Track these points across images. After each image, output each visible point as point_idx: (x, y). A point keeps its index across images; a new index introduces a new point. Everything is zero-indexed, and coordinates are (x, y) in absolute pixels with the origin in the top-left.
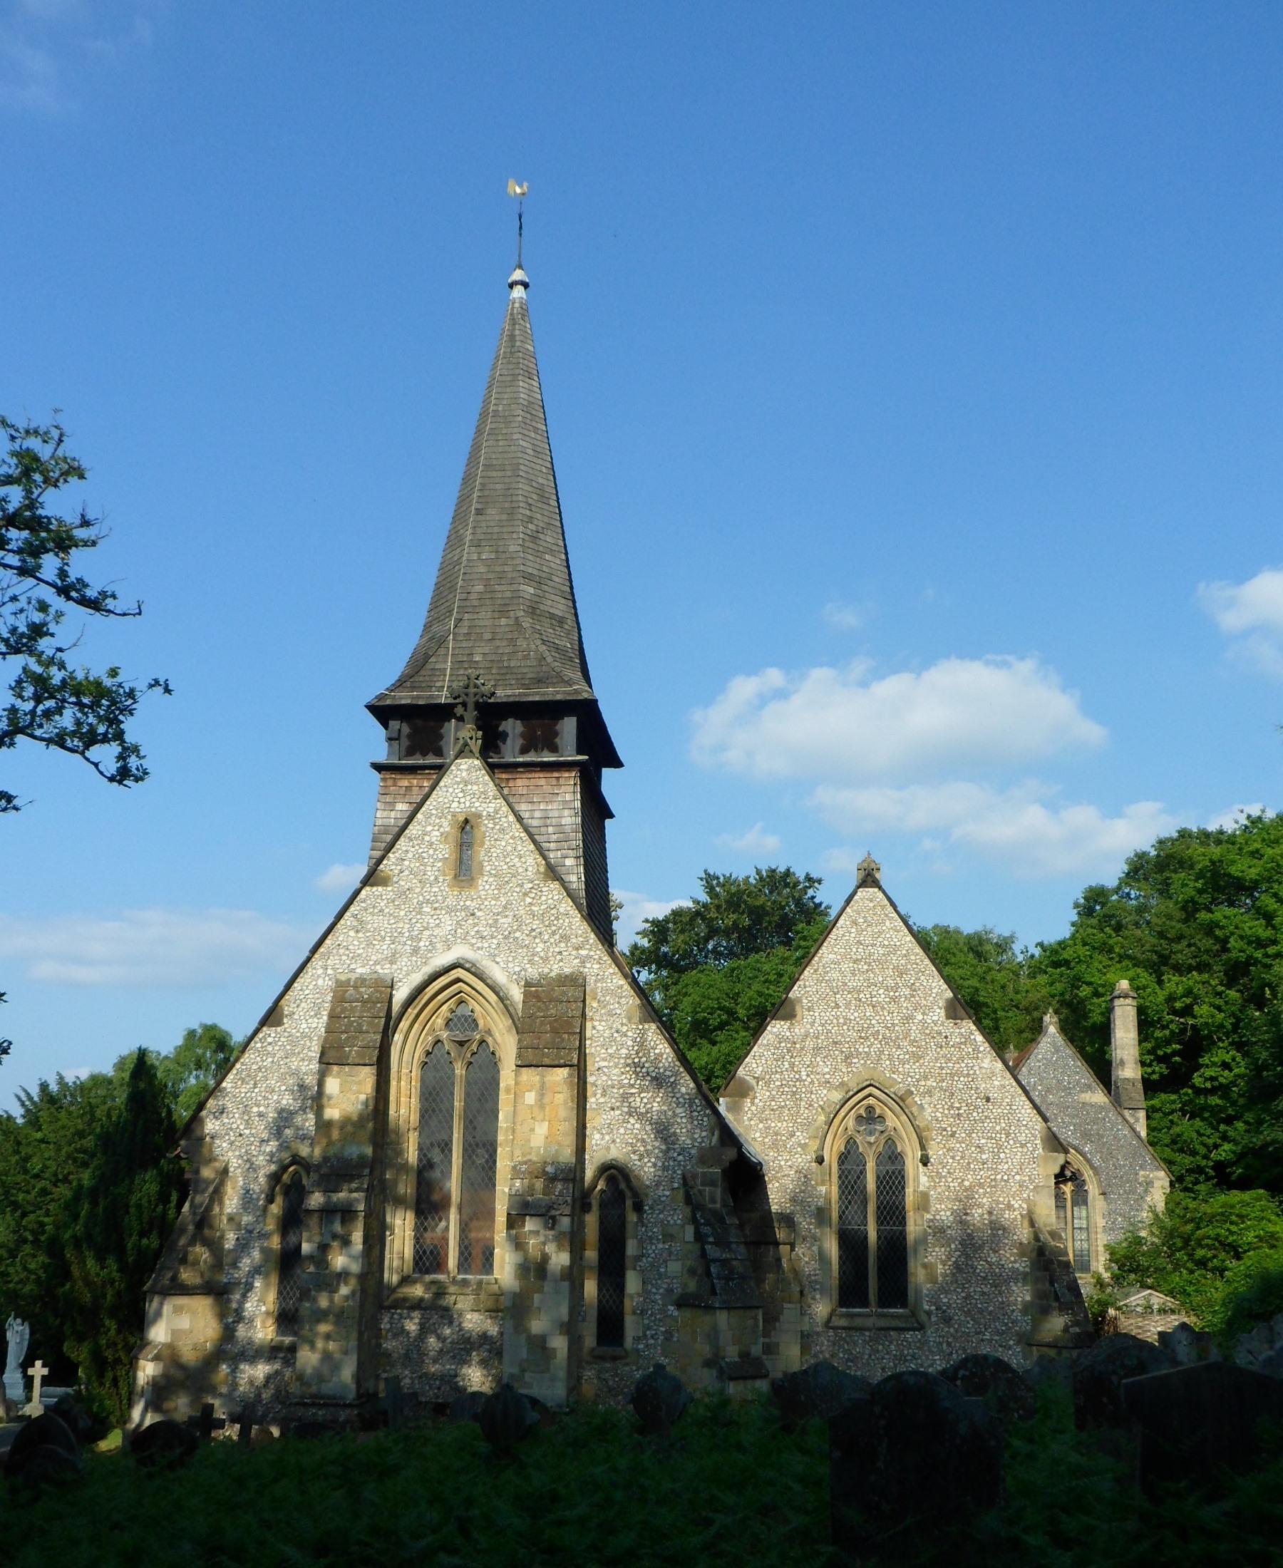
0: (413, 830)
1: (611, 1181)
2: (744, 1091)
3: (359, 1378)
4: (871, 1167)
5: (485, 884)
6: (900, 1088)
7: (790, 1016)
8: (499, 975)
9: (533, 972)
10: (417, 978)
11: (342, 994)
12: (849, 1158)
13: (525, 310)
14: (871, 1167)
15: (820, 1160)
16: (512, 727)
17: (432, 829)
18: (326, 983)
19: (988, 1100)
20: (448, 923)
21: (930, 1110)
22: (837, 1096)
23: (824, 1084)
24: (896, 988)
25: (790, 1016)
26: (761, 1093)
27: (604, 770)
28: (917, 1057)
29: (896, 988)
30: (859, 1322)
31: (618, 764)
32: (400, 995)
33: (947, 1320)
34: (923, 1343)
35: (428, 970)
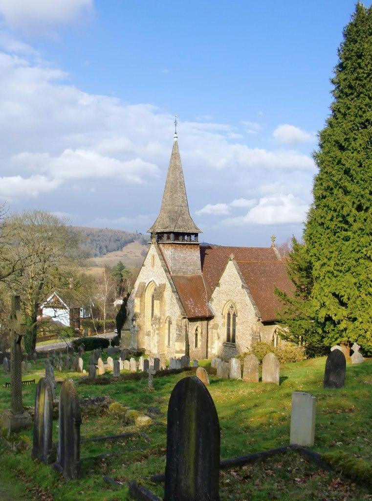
1: (170, 319)
2: (212, 300)
4: (232, 316)
6: (234, 302)
7: (219, 286)
8: (157, 283)
9: (160, 283)
10: (148, 283)
12: (229, 314)
13: (176, 142)
14: (232, 316)
16: (165, 235)
18: (139, 283)
19: (247, 305)
21: (238, 306)
22: (225, 302)
25: (219, 286)
26: (215, 300)
30: (228, 345)
32: (146, 285)
35: (149, 281)
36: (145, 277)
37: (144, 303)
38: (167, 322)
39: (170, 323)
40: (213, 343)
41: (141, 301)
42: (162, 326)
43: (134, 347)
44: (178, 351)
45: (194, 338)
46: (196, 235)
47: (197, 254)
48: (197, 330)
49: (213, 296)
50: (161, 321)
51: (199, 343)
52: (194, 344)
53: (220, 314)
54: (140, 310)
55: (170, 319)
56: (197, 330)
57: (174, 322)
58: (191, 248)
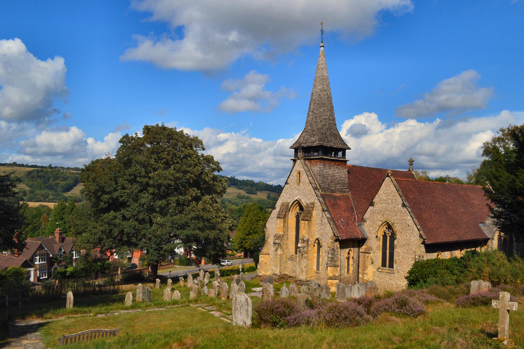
0: (292, 174)
3: (280, 272)
4: (388, 238)
5: (301, 184)
7: (373, 205)
10: (292, 202)
11: (283, 205)
12: (385, 236)
15: (377, 237)
17: (294, 173)
18: (281, 202)
20: (297, 191)
21: (397, 228)
23: (379, 219)
24: (392, 200)
25: (373, 205)
26: (368, 222)
27: (347, 151)
28: (396, 215)
29: (392, 200)
31: (350, 149)
32: (290, 205)
33: (399, 272)
34: (394, 277)
35: (294, 200)
36: (288, 196)
37: (288, 224)
38: (316, 245)
39: (319, 246)
40: (365, 268)
41: (284, 222)
42: (310, 249)
43: (276, 273)
44: (331, 277)
45: (346, 263)
46: (344, 151)
47: (345, 171)
48: (349, 253)
49: (367, 216)
50: (310, 243)
51: (351, 268)
52: (346, 270)
53: (374, 236)
54: (284, 232)
55: (319, 241)
56: (349, 253)
57: (324, 244)
58: (339, 165)
